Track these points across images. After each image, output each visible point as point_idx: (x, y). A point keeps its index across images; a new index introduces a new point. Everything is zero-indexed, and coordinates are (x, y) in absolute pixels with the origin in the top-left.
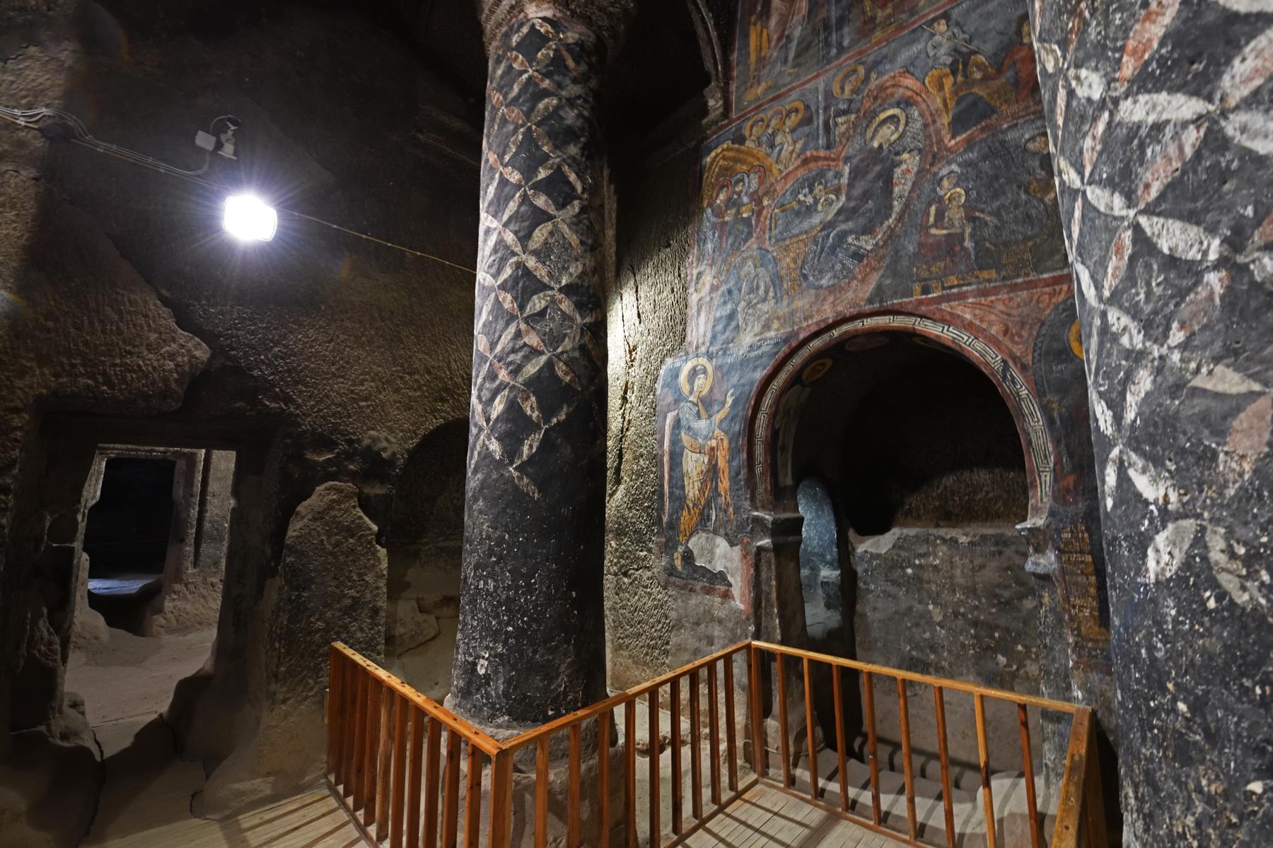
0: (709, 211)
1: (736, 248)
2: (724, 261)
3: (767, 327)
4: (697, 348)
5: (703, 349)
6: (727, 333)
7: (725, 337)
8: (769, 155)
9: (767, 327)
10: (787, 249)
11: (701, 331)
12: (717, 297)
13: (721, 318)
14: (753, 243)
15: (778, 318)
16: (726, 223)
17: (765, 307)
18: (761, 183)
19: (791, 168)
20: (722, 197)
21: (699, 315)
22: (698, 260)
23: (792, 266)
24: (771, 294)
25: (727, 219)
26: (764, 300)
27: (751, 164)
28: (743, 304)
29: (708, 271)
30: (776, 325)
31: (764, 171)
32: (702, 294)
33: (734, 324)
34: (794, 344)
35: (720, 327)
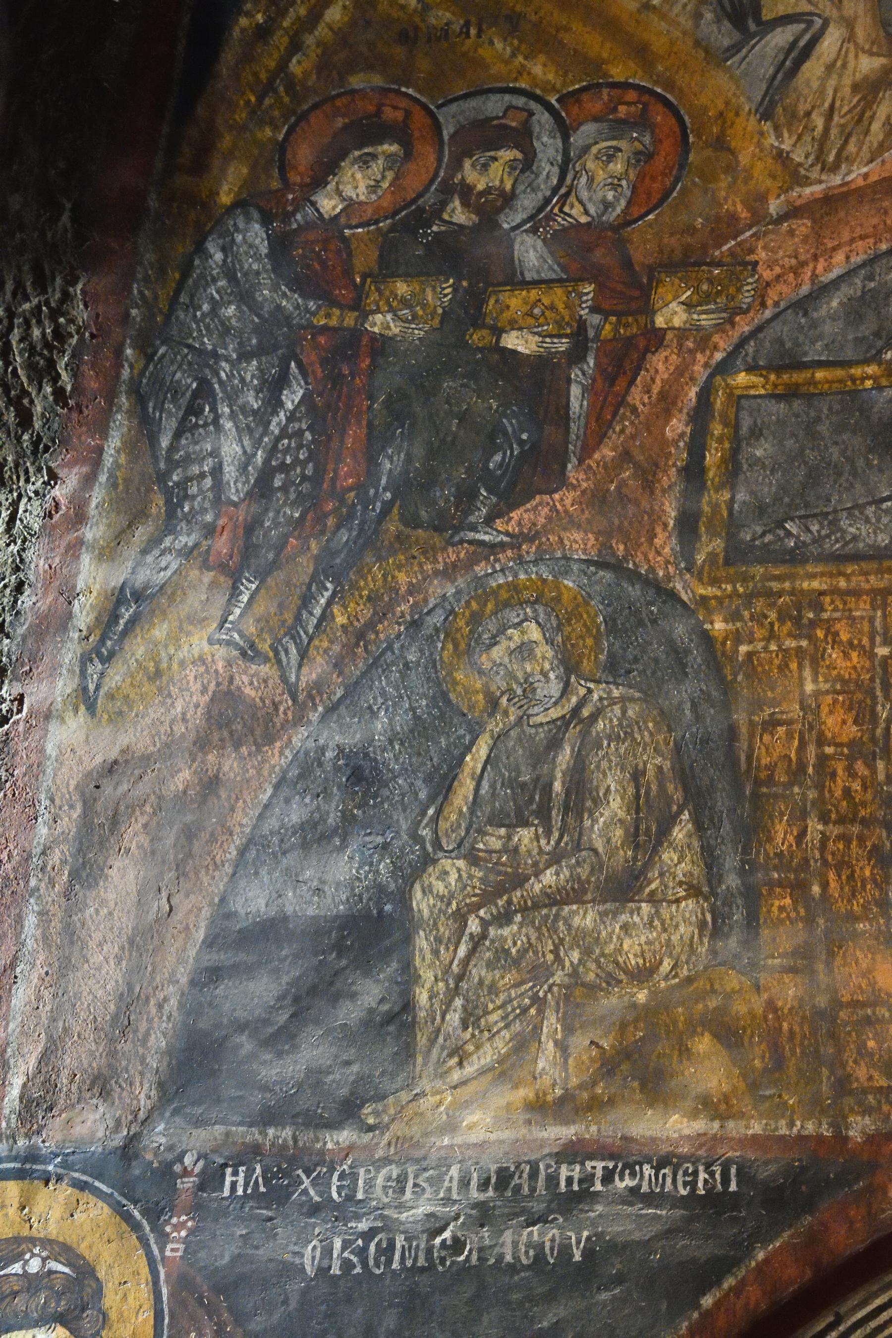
0: (254, 236)
1: (434, 512)
2: (336, 571)
3: (638, 1064)
4: (36, 1106)
5: (92, 1125)
6: (313, 1052)
7: (283, 1070)
8: (717, 58)
9: (638, 1064)
10: (803, 614)
11: (101, 977)
12: (255, 783)
13: (269, 931)
14: (561, 523)
15: (729, 1034)
16: (381, 346)
17: (632, 935)
18: (648, 194)
19: (857, 174)
20: (357, 184)
21: (85, 872)
22: (130, 510)
23: (838, 724)
24: (678, 859)
25: (380, 323)
26: (623, 888)
27: (597, 66)
28: (450, 876)
29: (201, 592)
30: (709, 1069)
31: (675, 141)
32: (135, 737)
33: (371, 993)
34: (846, 1239)
35: (258, 992)
